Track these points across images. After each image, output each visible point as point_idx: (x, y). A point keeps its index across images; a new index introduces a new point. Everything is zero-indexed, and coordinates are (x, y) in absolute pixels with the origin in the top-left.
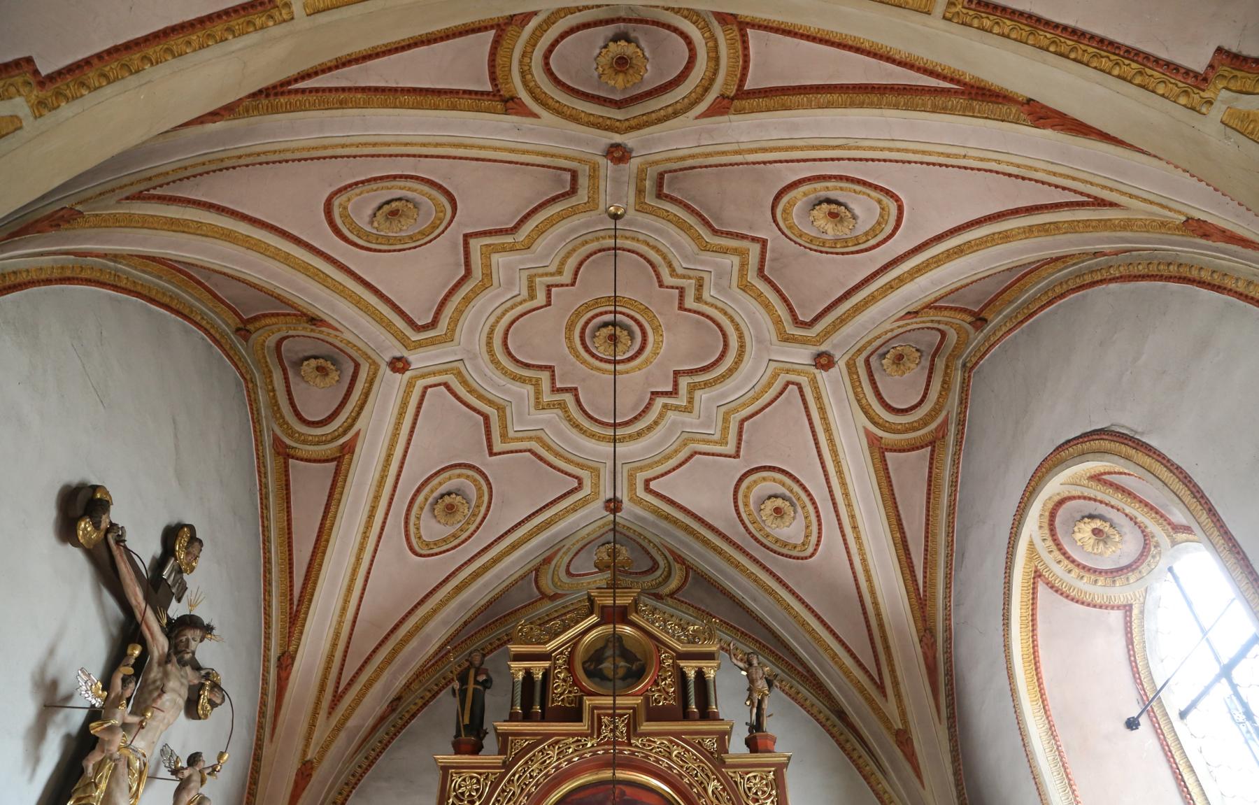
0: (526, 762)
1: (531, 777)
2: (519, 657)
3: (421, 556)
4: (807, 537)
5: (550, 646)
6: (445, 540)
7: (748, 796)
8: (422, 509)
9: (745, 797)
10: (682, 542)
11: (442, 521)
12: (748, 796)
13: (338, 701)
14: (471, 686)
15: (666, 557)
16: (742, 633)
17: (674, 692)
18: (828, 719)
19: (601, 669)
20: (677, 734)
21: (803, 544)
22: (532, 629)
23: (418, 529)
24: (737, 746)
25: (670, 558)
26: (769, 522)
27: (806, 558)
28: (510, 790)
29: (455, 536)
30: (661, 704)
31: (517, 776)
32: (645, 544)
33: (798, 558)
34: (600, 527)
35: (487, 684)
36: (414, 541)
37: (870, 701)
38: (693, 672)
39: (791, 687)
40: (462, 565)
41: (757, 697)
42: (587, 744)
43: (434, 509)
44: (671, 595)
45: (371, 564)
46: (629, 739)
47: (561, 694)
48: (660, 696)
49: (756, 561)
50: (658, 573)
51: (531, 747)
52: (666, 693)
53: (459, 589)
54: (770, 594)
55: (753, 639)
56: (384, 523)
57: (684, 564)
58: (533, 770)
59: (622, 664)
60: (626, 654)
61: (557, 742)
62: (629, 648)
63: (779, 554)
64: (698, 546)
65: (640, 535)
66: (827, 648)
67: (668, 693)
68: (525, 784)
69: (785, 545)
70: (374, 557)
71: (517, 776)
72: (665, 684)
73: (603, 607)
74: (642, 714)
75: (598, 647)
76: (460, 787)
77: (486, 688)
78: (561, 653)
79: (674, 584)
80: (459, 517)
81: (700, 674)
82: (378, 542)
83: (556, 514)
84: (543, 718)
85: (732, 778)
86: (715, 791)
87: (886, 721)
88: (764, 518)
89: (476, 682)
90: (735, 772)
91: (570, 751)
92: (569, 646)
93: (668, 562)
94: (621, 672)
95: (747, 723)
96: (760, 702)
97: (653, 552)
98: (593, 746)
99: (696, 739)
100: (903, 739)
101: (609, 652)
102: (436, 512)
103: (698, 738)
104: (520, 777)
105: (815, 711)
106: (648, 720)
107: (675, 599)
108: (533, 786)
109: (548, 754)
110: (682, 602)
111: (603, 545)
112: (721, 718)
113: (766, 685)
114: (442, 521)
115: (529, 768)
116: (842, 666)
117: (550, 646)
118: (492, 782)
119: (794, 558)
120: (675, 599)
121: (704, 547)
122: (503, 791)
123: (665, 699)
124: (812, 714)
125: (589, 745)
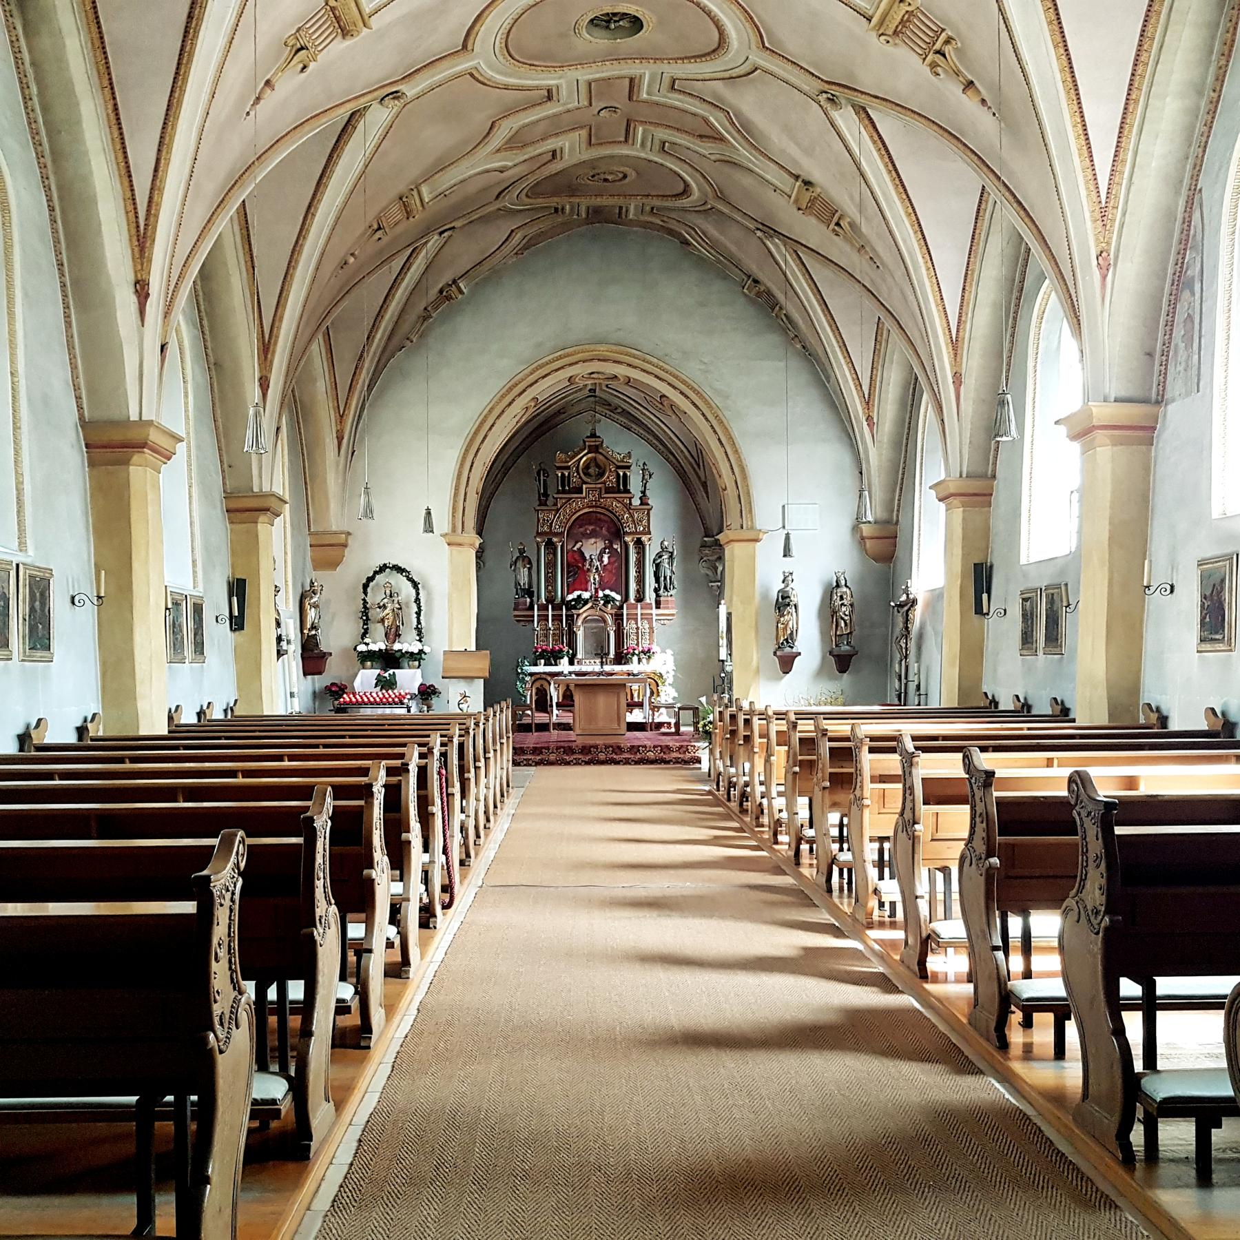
2: (559, 468)
20: (615, 498)
24: (636, 502)
37: (694, 469)
51: (566, 503)
60: (598, 466)
66: (679, 448)
73: (589, 446)
74: (603, 491)
81: (625, 474)
84: (569, 492)
89: (544, 476)
103: (621, 500)
106: (606, 493)
117: (570, 464)
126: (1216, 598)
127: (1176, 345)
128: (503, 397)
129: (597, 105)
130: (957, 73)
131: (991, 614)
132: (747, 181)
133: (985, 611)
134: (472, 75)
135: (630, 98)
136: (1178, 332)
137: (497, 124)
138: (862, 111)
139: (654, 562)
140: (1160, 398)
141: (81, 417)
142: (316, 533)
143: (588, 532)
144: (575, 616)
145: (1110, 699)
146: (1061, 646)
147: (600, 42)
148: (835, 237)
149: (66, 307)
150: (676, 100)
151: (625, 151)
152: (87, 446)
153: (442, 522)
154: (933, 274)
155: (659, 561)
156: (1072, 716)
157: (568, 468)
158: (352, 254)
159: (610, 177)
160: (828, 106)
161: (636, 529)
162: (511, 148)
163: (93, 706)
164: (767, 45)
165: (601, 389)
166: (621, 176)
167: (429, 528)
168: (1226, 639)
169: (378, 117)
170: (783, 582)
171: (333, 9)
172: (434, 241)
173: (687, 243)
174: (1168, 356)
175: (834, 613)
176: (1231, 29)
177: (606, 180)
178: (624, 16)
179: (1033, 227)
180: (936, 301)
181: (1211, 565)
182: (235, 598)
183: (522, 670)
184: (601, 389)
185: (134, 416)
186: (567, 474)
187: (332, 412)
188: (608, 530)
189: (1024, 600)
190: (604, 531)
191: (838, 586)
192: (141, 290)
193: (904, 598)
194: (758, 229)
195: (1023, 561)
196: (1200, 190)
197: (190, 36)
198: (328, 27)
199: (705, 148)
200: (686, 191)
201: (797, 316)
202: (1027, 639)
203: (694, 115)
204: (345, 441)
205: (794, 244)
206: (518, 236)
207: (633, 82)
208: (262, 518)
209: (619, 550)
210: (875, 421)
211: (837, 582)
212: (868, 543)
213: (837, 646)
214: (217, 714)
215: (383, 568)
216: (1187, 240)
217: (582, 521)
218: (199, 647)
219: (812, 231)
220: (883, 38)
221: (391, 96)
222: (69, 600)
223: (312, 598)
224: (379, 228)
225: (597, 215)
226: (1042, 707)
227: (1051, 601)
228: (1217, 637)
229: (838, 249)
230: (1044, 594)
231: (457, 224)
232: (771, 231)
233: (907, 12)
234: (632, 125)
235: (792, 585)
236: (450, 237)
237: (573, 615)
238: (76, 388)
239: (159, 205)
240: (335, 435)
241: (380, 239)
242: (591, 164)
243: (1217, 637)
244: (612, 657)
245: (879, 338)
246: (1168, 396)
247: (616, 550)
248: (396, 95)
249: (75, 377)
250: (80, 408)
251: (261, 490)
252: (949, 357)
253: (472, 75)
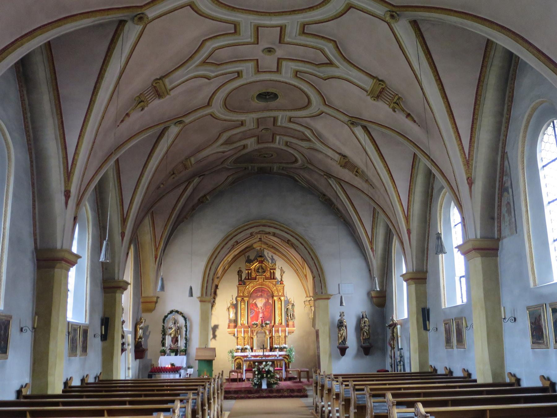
14: (240, 274)
20: (270, 282)
35: (242, 273)
51: (250, 283)
52: (268, 275)
60: (262, 268)
73: (259, 261)
84: (251, 279)
87: (304, 273)
100: (306, 276)
117: (251, 268)
126: (537, 324)
127: (504, 215)
128: (223, 241)
129: (261, 128)
130: (403, 110)
131: (431, 330)
132: (320, 156)
133: (428, 329)
134: (211, 115)
135: (274, 125)
136: (504, 209)
137: (221, 134)
138: (365, 128)
140: (499, 236)
141: (36, 248)
142: (144, 297)
145: (492, 371)
146: (464, 345)
147: (262, 104)
148: (356, 177)
149: (34, 201)
150: (291, 125)
151: (272, 145)
152: (37, 260)
153: (197, 292)
154: (396, 190)
155: (288, 307)
156: (473, 377)
157: (251, 269)
158: (162, 184)
159: (266, 156)
160: (352, 126)
162: (227, 144)
163: (26, 379)
164: (327, 103)
165: (264, 238)
166: (270, 155)
167: (191, 295)
168: (545, 342)
169: (174, 130)
170: (340, 316)
171: (155, 87)
172: (196, 180)
173: (297, 181)
174: (500, 219)
175: (362, 329)
176: (512, 91)
177: (265, 157)
178: (272, 93)
179: (438, 169)
180: (398, 201)
181: (533, 309)
182: (103, 327)
184: (264, 238)
185: (59, 246)
186: (250, 272)
187: (153, 247)
188: (267, 294)
189: (446, 324)
190: (265, 295)
191: (363, 317)
192: (67, 194)
193: (392, 322)
194: (325, 175)
195: (443, 307)
196: (507, 152)
197: (95, 95)
198: (151, 92)
199: (304, 144)
200: (296, 161)
201: (341, 208)
202: (448, 341)
203: (299, 131)
204: (158, 259)
205: (339, 181)
206: (230, 178)
207: (275, 119)
208: (118, 291)
209: (271, 303)
210: (374, 249)
211: (362, 316)
212: (374, 300)
213: (363, 343)
214: (91, 380)
215: (172, 312)
216: (503, 172)
217: (256, 291)
218: (85, 349)
219: (346, 175)
220: (373, 98)
221: (179, 122)
222: (19, 329)
223: (140, 325)
224: (174, 174)
225: (262, 171)
226: (458, 373)
227: (458, 325)
228: (540, 342)
229: (358, 182)
230: (454, 322)
231: (206, 173)
232: (329, 175)
233: (382, 88)
234: (275, 135)
235: (344, 318)
236: (203, 178)
238: (35, 235)
239: (77, 160)
240: (154, 256)
241: (174, 178)
242: (259, 150)
243: (540, 342)
245: (374, 216)
246: (503, 235)
247: (270, 303)
248: (180, 122)
249: (35, 231)
250: (35, 243)
251: (119, 279)
252: (405, 223)
253: (211, 115)
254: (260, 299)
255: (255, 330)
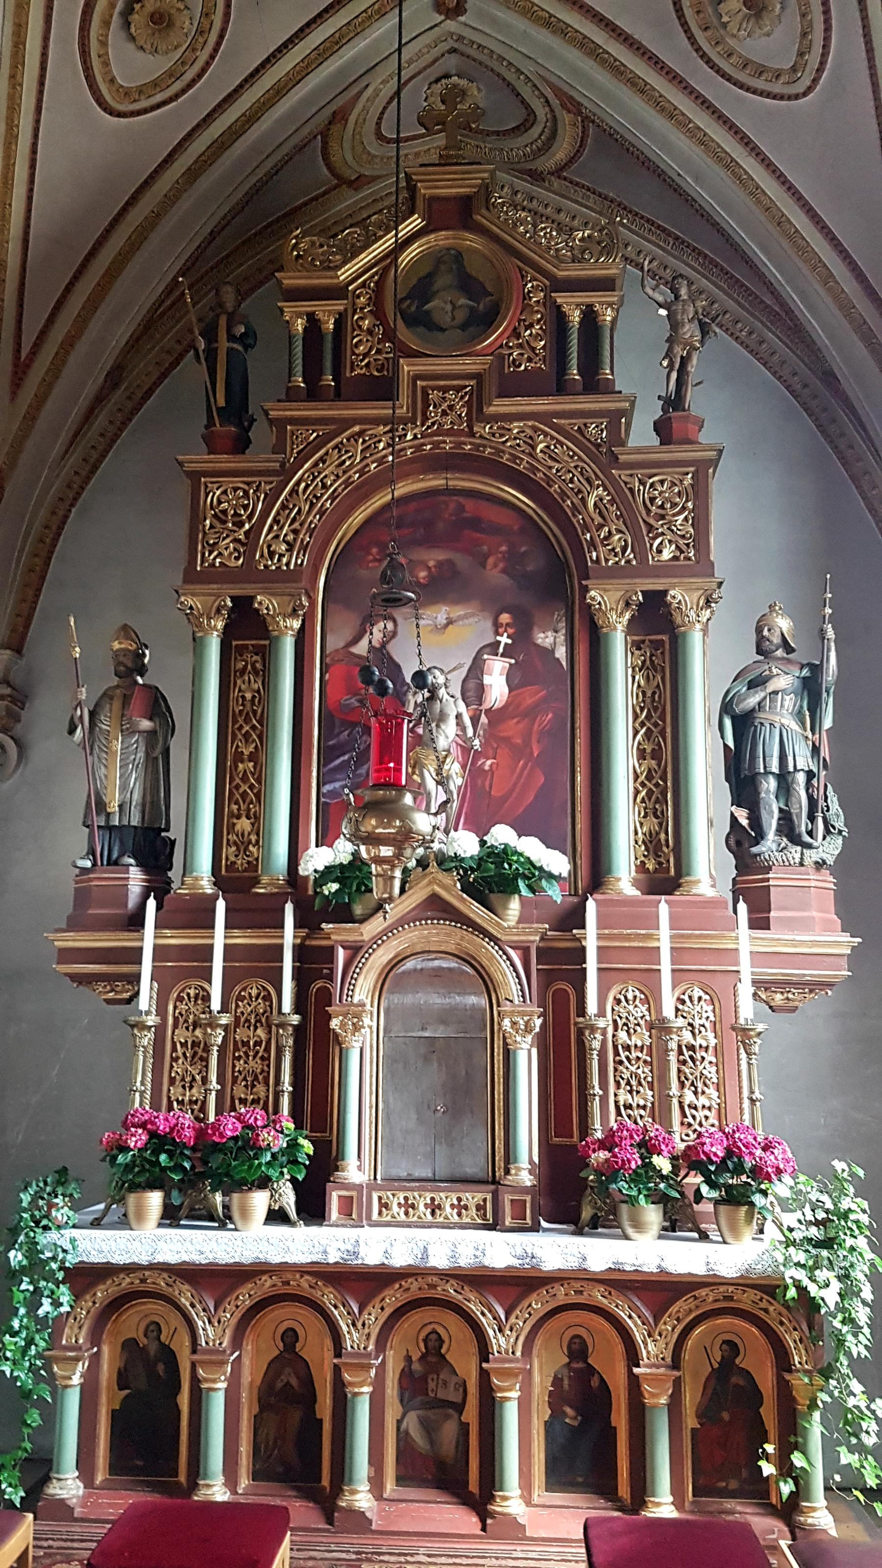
0: (316, 464)
1: (325, 487)
3: (120, 115)
4: (801, 54)
5: (344, 274)
6: (155, 84)
7: (648, 511)
8: (107, 24)
9: (644, 512)
10: (575, 71)
11: (148, 47)
12: (648, 511)
13: (24, 373)
14: (224, 344)
15: (547, 101)
16: (677, 238)
17: (544, 347)
18: (805, 386)
19: (428, 312)
20: (545, 418)
21: (794, 69)
22: (313, 243)
23: (106, 64)
25: (555, 102)
26: (733, 28)
27: (797, 97)
28: (294, 506)
29: (172, 75)
30: (522, 368)
31: (303, 485)
32: (510, 76)
33: (782, 98)
34: (428, 46)
35: (248, 340)
36: (104, 89)
38: (577, 313)
39: (750, 333)
40: (194, 130)
41: (679, 351)
42: (405, 435)
43: (129, 24)
44: (558, 172)
45: (36, 136)
46: (471, 427)
47: (365, 355)
48: (522, 354)
49: (705, 103)
50: (535, 131)
51: (322, 442)
53: (193, 174)
54: (727, 167)
55: (694, 249)
56: (44, 55)
57: (580, 113)
58: (326, 477)
59: (463, 301)
61: (361, 433)
62: (474, 273)
63: (748, 90)
64: (602, 77)
65: (501, 58)
66: (817, 264)
67: (533, 349)
68: (315, 496)
69: (760, 71)
70: (37, 121)
71: (303, 485)
72: (530, 335)
75: (422, 274)
76: (220, 502)
77: (246, 347)
78: (363, 285)
79: (560, 153)
80: (174, 37)
81: (590, 315)
82: (41, 92)
83: (349, 23)
84: (338, 395)
85: (626, 483)
86: (600, 504)
88: (725, 19)
89: (231, 338)
90: (631, 475)
91: (381, 446)
92: (376, 273)
93: (552, 111)
94: (461, 316)
95: (659, 397)
96: (684, 361)
97: (526, 92)
98: (415, 437)
99: (575, 424)
101: (440, 282)
102: (133, 30)
104: (307, 486)
105: (785, 372)
107: (565, 179)
108: (326, 500)
109: (347, 452)
110: (577, 184)
111: (437, 81)
112: (617, 389)
113: (698, 333)
114: (148, 47)
115: (319, 473)
116: (838, 295)
117: (344, 274)
118: (266, 495)
119: (775, 97)
120: (565, 179)
121: (615, 81)
122: (284, 507)
123: (530, 360)
124: (779, 378)
125: (409, 437)
139: (726, 707)
143: (423, 574)
144: (341, 955)
161: (641, 552)
183: (32, 1249)
209: (561, 653)
237: (329, 954)
244: (526, 1179)
254: (440, 613)
255: (355, 950)
